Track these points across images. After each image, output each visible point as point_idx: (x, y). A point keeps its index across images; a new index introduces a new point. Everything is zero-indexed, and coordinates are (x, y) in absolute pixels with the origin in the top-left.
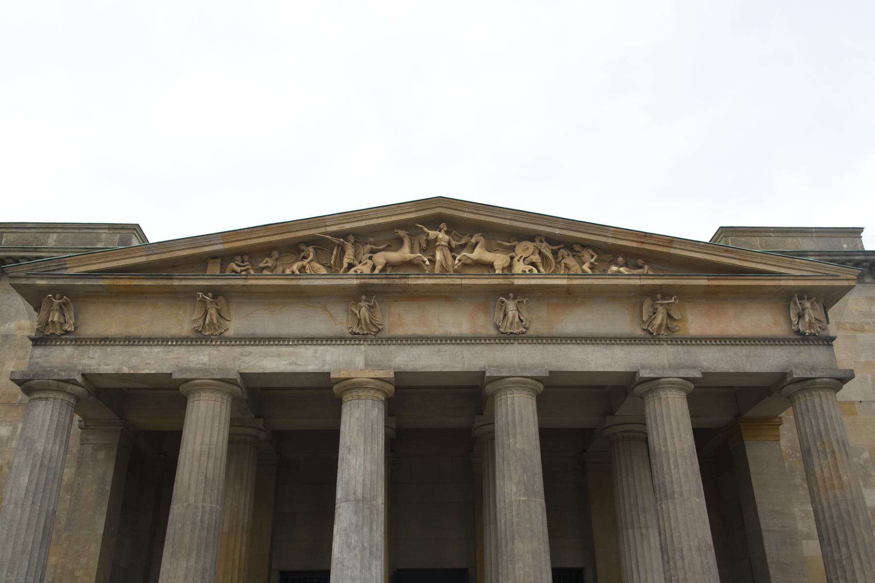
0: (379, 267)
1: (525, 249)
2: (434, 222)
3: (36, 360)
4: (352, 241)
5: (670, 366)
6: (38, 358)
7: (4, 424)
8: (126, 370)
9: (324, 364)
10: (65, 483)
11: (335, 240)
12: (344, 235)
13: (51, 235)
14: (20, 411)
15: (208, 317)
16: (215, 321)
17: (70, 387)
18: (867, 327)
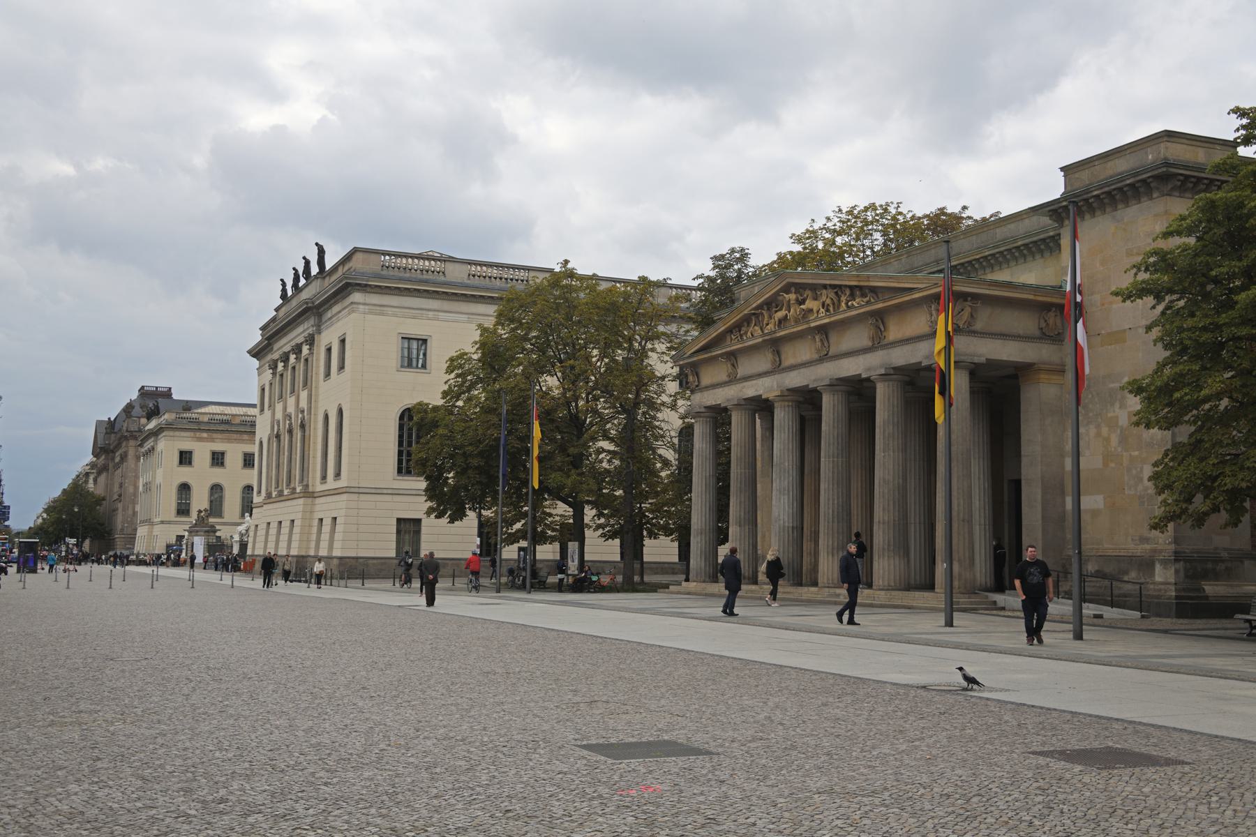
17: (702, 415)
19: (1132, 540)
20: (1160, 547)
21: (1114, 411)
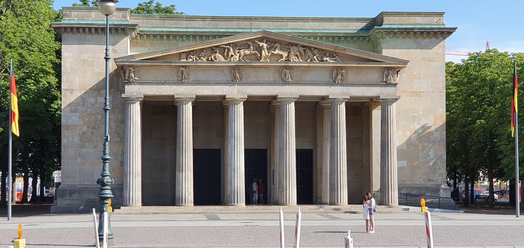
0: (242, 56)
1: (294, 50)
2: (261, 40)
3: (127, 90)
4: (232, 46)
5: (340, 93)
6: (128, 89)
7: (92, 97)
8: (158, 94)
9: (224, 91)
10: (119, 120)
11: (226, 47)
12: (229, 44)
13: (92, 12)
14: (97, 92)
15: (184, 75)
16: (186, 77)
18: (435, 59)
19: (423, 181)
20: (438, 183)
21: (414, 126)
